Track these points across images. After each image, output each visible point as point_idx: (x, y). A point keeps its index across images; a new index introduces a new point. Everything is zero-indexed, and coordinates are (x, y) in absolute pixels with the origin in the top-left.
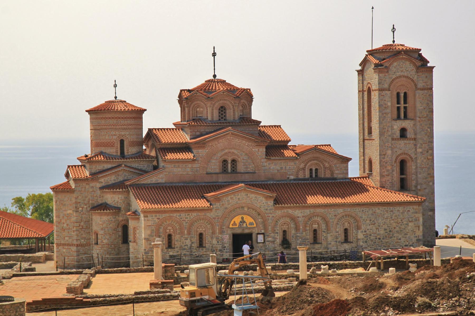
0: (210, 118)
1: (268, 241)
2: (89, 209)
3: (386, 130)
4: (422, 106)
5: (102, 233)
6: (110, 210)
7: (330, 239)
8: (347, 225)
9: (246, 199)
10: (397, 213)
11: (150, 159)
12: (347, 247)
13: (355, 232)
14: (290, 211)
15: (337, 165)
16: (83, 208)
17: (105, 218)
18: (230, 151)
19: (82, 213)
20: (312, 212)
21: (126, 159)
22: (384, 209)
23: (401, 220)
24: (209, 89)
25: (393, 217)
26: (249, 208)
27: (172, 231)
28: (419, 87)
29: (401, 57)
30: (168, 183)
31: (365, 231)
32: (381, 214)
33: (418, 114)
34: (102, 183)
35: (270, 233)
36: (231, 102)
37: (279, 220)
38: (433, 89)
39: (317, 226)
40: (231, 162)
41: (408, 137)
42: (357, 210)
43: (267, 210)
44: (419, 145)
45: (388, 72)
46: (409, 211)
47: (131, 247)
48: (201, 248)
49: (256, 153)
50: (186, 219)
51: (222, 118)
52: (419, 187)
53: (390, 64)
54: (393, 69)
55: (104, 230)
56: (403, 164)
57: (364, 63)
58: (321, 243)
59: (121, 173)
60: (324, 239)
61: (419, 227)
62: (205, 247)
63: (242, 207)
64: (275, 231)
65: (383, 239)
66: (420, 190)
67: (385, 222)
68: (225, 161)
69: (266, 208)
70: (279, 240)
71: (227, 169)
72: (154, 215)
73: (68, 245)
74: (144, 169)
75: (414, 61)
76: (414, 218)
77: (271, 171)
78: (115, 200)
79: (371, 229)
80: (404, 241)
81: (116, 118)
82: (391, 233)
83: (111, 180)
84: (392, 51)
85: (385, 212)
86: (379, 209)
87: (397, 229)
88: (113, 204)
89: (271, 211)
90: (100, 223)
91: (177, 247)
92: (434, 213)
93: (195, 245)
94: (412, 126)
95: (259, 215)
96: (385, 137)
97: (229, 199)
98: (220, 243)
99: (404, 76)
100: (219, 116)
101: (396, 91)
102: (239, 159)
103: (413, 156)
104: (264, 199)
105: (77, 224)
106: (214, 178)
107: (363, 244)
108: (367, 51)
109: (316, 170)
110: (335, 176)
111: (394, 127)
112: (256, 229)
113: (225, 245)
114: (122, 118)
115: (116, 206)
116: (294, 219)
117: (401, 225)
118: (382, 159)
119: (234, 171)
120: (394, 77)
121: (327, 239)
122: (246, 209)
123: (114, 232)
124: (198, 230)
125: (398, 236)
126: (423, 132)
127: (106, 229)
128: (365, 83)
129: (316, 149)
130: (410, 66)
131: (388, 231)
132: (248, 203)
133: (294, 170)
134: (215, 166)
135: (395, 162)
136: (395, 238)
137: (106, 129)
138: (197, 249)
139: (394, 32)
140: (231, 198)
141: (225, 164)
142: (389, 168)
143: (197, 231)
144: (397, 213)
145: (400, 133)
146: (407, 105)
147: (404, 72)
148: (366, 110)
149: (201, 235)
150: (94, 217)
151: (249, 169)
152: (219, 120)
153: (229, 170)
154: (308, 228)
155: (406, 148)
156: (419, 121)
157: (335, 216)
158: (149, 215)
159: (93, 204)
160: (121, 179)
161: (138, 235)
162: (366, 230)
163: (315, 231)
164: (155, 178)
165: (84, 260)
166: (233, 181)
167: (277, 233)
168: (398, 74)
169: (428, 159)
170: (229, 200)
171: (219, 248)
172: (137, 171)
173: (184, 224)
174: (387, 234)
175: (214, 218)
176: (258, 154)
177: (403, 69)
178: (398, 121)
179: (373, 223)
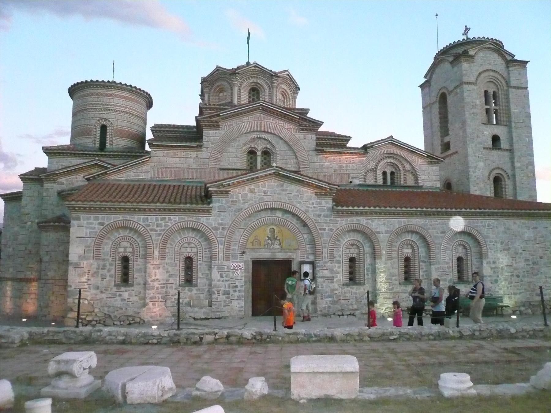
0: (236, 102)
1: (322, 277)
5: (47, 260)
9: (279, 194)
14: (363, 220)
16: (32, 222)
25: (538, 239)
29: (488, 46)
34: (62, 184)
35: (326, 262)
36: (267, 82)
37: (342, 238)
38: (528, 89)
43: (320, 216)
48: (187, 288)
49: (301, 141)
50: (157, 227)
60: (423, 276)
62: (196, 285)
68: (252, 153)
69: (318, 213)
70: (342, 275)
72: (92, 216)
77: (325, 170)
83: (77, 181)
86: (515, 223)
89: (328, 219)
90: (46, 243)
98: (225, 278)
99: (492, 71)
103: (509, 172)
105: (22, 248)
107: (491, 285)
109: (392, 173)
110: (421, 183)
120: (481, 70)
127: (53, 253)
129: (391, 140)
131: (530, 263)
132: (282, 201)
133: (359, 171)
136: (544, 276)
138: (181, 288)
140: (250, 190)
151: (290, 166)
155: (500, 161)
157: (443, 232)
158: (81, 216)
170: (246, 194)
171: (223, 289)
173: (153, 237)
174: (528, 267)
175: (216, 229)
176: (305, 142)
178: (488, 126)
179: (507, 247)
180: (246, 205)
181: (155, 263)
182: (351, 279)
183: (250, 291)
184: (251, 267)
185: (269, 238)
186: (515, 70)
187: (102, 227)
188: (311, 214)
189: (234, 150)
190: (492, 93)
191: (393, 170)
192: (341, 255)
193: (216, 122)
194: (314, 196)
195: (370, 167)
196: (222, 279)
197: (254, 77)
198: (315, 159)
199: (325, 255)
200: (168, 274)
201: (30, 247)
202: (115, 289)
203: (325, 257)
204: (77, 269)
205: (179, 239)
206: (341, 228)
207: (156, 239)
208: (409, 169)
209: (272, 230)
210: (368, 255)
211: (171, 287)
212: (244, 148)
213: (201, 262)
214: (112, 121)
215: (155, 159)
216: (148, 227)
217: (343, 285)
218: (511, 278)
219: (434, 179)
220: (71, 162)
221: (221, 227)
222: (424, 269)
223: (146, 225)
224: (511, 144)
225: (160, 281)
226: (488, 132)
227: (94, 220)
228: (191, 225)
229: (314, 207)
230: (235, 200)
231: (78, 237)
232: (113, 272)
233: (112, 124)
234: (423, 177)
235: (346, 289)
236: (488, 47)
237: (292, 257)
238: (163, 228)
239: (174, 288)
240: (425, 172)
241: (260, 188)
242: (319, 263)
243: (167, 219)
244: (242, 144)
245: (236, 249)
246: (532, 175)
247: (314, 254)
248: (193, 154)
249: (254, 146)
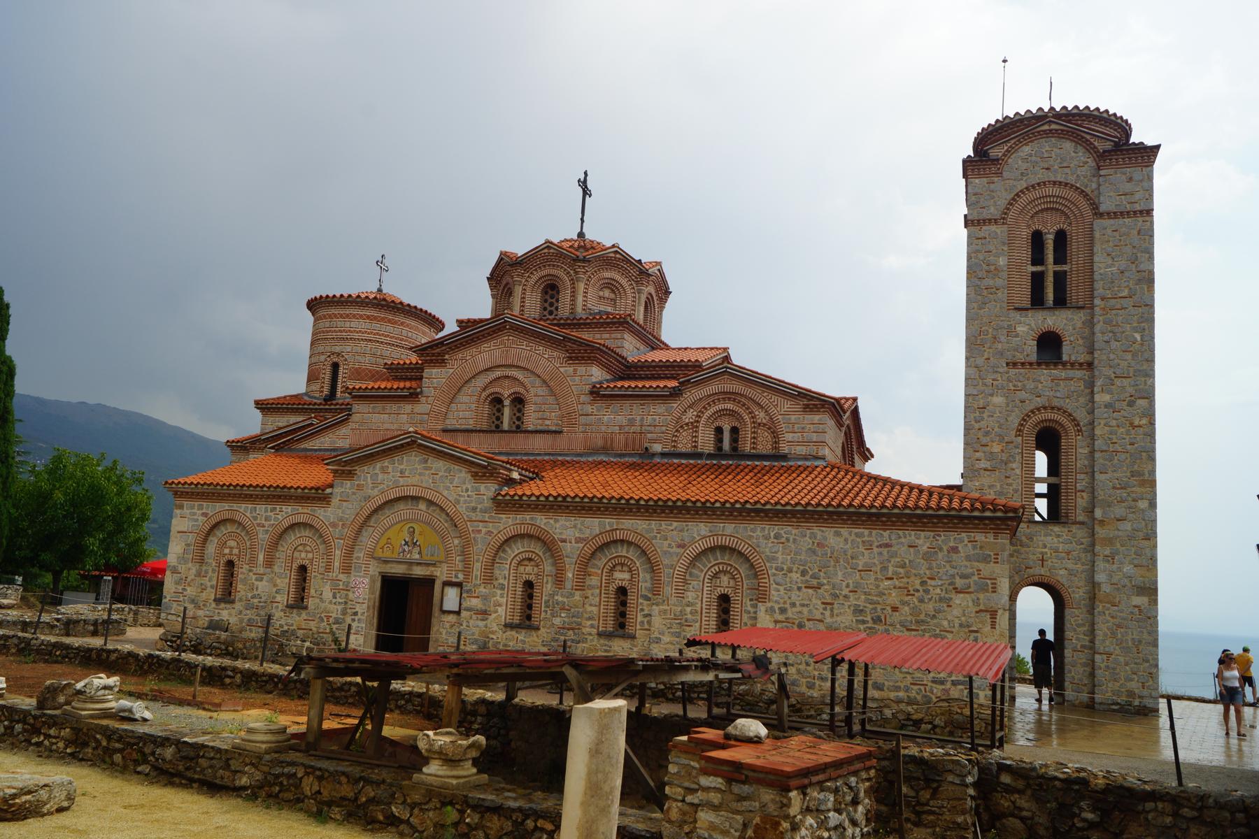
3: (990, 336)
7: (657, 621)
13: (752, 610)
14: (542, 520)
15: (793, 417)
20: (608, 528)
22: (857, 535)
23: (923, 583)
25: (891, 569)
27: (236, 551)
28: (1103, 208)
29: (1046, 127)
31: (783, 611)
32: (845, 552)
42: (758, 533)
43: (474, 509)
44: (1099, 383)
45: (999, 174)
46: (954, 550)
52: (1098, 513)
53: (1007, 151)
58: (633, 637)
60: (642, 622)
61: (993, 614)
62: (306, 608)
66: (1102, 522)
67: (857, 585)
69: (473, 505)
72: (196, 503)
75: (1088, 137)
76: (976, 578)
77: (603, 428)
79: (803, 605)
85: (862, 549)
86: (838, 534)
89: (487, 515)
91: (241, 600)
92: (1154, 602)
93: (282, 599)
94: (1079, 324)
96: (986, 356)
97: (376, 472)
101: (1029, 226)
103: (1081, 415)
104: (469, 476)
109: (734, 430)
110: (785, 449)
111: (1018, 329)
112: (445, 566)
113: (358, 608)
114: (341, 316)
116: (549, 545)
117: (921, 601)
118: (973, 423)
120: (1022, 185)
121: (649, 623)
124: (296, 554)
126: (1114, 344)
130: (1075, 152)
131: (869, 618)
132: (424, 485)
133: (664, 428)
135: (1019, 432)
138: (288, 610)
140: (382, 468)
142: (996, 448)
146: (1065, 268)
151: (548, 422)
153: (506, 426)
154: (594, 581)
157: (679, 546)
158: (185, 503)
162: (787, 606)
163: (622, 591)
167: (502, 587)
169: (1134, 427)
171: (334, 615)
173: (260, 536)
175: (334, 525)
178: (1030, 313)
179: (815, 582)
180: (376, 492)
181: (258, 572)
183: (375, 621)
184: (378, 585)
186: (1116, 173)
187: (206, 519)
188: (462, 507)
189: (465, 399)
191: (736, 424)
192: (507, 576)
194: (470, 477)
195: (687, 421)
196: (334, 601)
197: (549, 265)
198: (589, 409)
202: (214, 605)
203: (476, 576)
204: (175, 575)
205: (293, 538)
206: (505, 531)
207: (263, 537)
208: (764, 421)
209: (412, 530)
210: (550, 578)
212: (483, 395)
213: (316, 574)
214: (346, 357)
216: (255, 520)
217: (506, 626)
219: (814, 440)
221: (341, 523)
222: (646, 612)
223: (253, 517)
225: (261, 598)
226: (1030, 325)
227: (198, 509)
228: (301, 519)
229: (468, 496)
230: (362, 482)
231: (179, 532)
232: (214, 583)
233: (346, 360)
237: (435, 574)
238: (272, 522)
239: (280, 608)
240: (796, 426)
241: (396, 465)
242: (466, 586)
243: (278, 509)
244: (479, 389)
245: (360, 557)
246: (1144, 421)
248: (408, 408)
249: (497, 390)
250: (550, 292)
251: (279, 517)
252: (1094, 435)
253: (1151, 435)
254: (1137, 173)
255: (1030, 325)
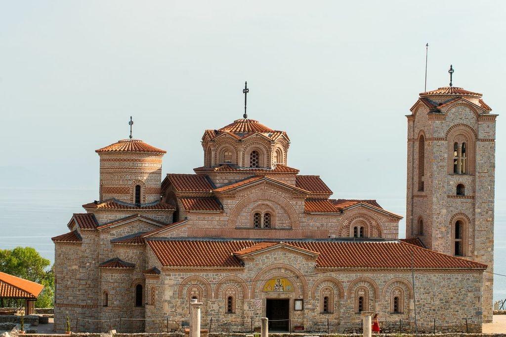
0: (240, 164)
1: (307, 309)
2: (97, 265)
4: (482, 160)
5: (113, 294)
6: (123, 267)
8: (397, 294)
10: (455, 282)
11: (170, 210)
12: (396, 318)
14: (334, 275)
15: (386, 224)
16: (90, 263)
17: (117, 276)
18: (265, 203)
19: (89, 269)
21: (143, 208)
24: (240, 131)
26: (286, 269)
27: (197, 292)
29: (461, 102)
30: (191, 238)
31: (418, 301)
33: (478, 169)
34: (114, 235)
39: (363, 293)
40: (265, 217)
41: (466, 194)
43: (307, 272)
44: (477, 205)
45: (444, 119)
46: (468, 279)
47: (147, 310)
51: (254, 164)
52: (476, 253)
54: (450, 115)
55: (115, 289)
56: (458, 225)
57: (415, 108)
59: (135, 224)
62: (235, 313)
63: (279, 268)
64: (315, 297)
65: (438, 310)
68: (257, 215)
70: (319, 308)
71: (260, 224)
73: (72, 305)
74: (162, 220)
78: (128, 256)
80: (462, 314)
81: (132, 160)
82: (448, 304)
83: (124, 232)
84: (451, 95)
86: (435, 276)
87: (455, 299)
88: (126, 260)
94: (470, 182)
95: (298, 278)
100: (251, 162)
102: (274, 213)
103: (470, 216)
104: (304, 260)
105: (83, 282)
106: (244, 234)
108: (420, 95)
109: (362, 228)
110: (384, 236)
115: (130, 262)
116: (337, 284)
117: (459, 295)
119: (268, 225)
120: (452, 124)
122: (283, 271)
123: (127, 292)
125: (455, 308)
126: (482, 190)
128: (417, 131)
133: (336, 228)
134: (246, 219)
136: (452, 310)
137: (120, 172)
139: (451, 73)
141: (257, 218)
142: (443, 230)
143: (226, 295)
144: (455, 282)
145: (457, 189)
147: (464, 120)
148: (417, 162)
149: (230, 298)
150: (104, 274)
152: (251, 166)
154: (353, 295)
156: (479, 177)
157: (384, 282)
159: (103, 259)
160: (136, 231)
161: (156, 297)
164: (177, 231)
165: (89, 323)
166: (266, 237)
168: (457, 122)
171: (250, 315)
172: (155, 223)
177: (462, 116)
182: (325, 310)
185: (277, 286)
189: (245, 214)
190: (461, 146)
193: (233, 194)
198: (304, 220)
199: (310, 295)
200: (219, 307)
201: (89, 282)
211: (221, 314)
215: (190, 222)
217: (320, 313)
218: (429, 312)
220: (116, 217)
224: (474, 192)
226: (454, 181)
228: (232, 278)
234: (385, 232)
235: (322, 316)
236: (460, 103)
246: (491, 219)
247: (304, 293)
248: (217, 218)
250: (253, 154)
251: (220, 278)
252: (475, 224)
253: (492, 224)
254: (490, 124)
255: (454, 181)
